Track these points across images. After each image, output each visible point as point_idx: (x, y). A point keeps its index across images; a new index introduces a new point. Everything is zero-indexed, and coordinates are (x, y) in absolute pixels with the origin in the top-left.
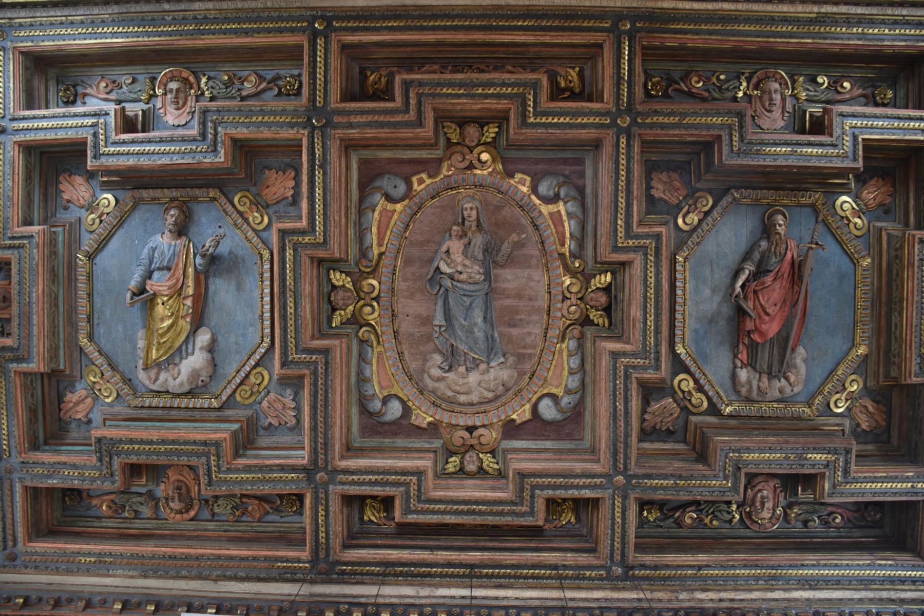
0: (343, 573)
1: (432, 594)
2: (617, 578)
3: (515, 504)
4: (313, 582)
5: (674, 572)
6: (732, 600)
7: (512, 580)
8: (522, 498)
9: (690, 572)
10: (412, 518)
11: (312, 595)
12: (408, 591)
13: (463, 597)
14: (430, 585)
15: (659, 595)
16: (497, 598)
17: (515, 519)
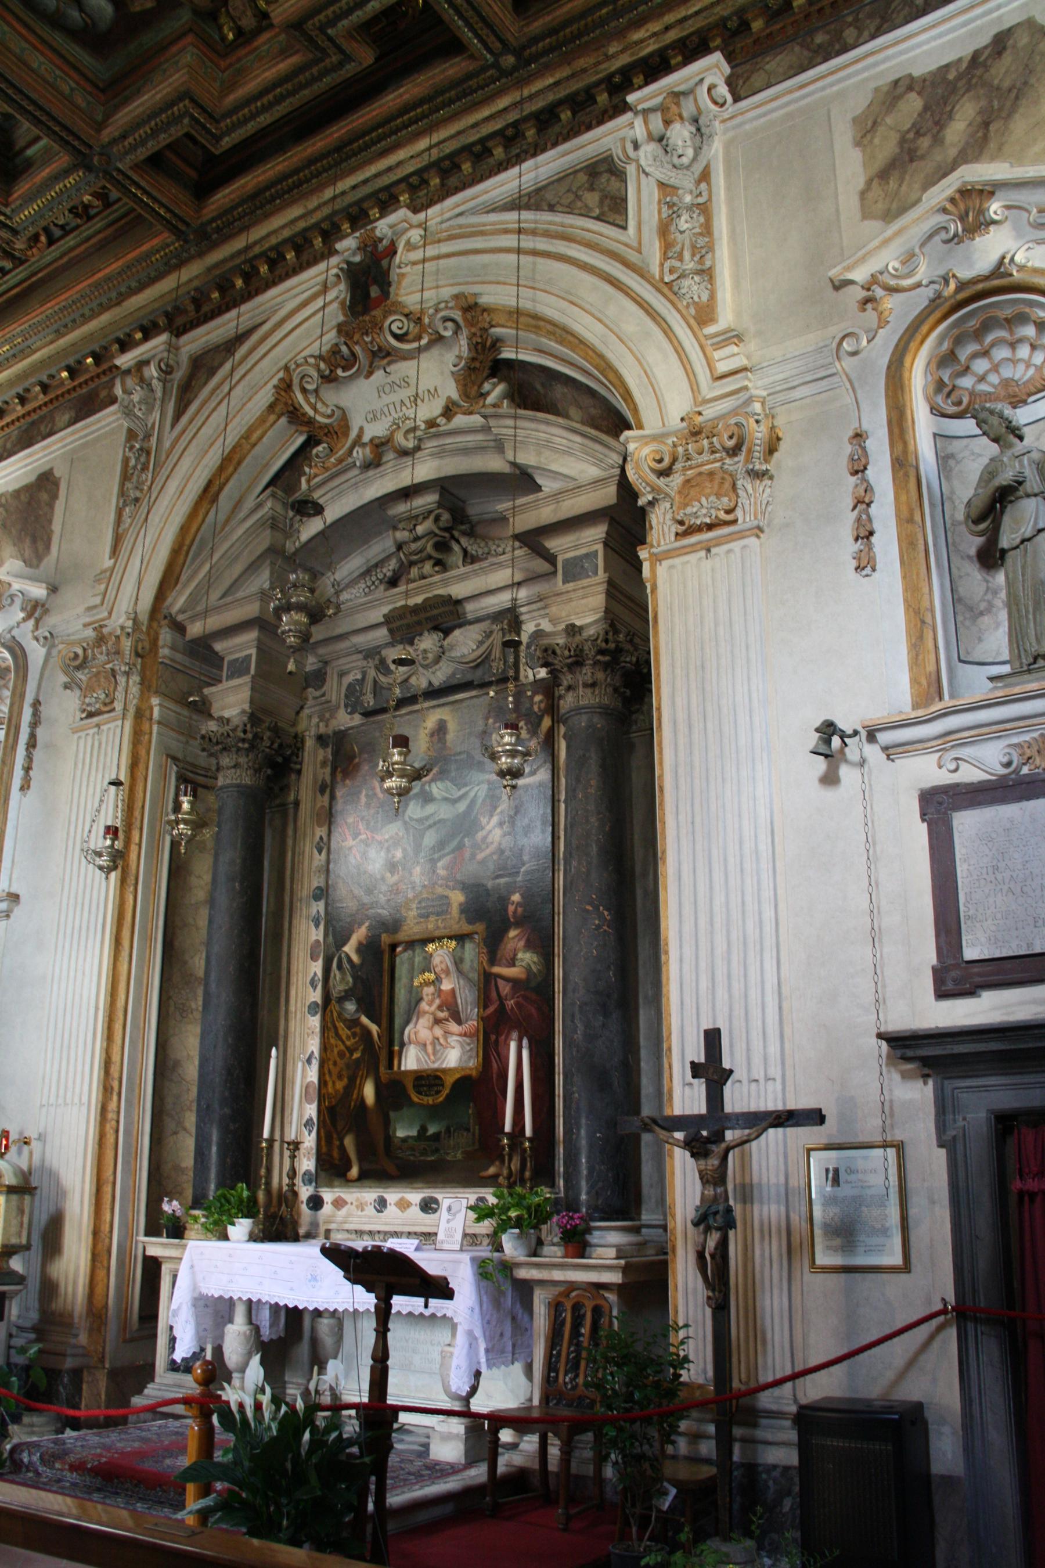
0: (218, 230)
1: (321, 201)
2: (515, 68)
3: (322, 60)
4: (201, 254)
5: (583, 22)
6: (685, 19)
7: (394, 137)
8: (323, 50)
9: (604, 11)
10: (227, 142)
11: (209, 269)
12: (295, 211)
13: (354, 187)
14: (312, 192)
15: (582, 63)
16: (390, 169)
17: (334, 75)
